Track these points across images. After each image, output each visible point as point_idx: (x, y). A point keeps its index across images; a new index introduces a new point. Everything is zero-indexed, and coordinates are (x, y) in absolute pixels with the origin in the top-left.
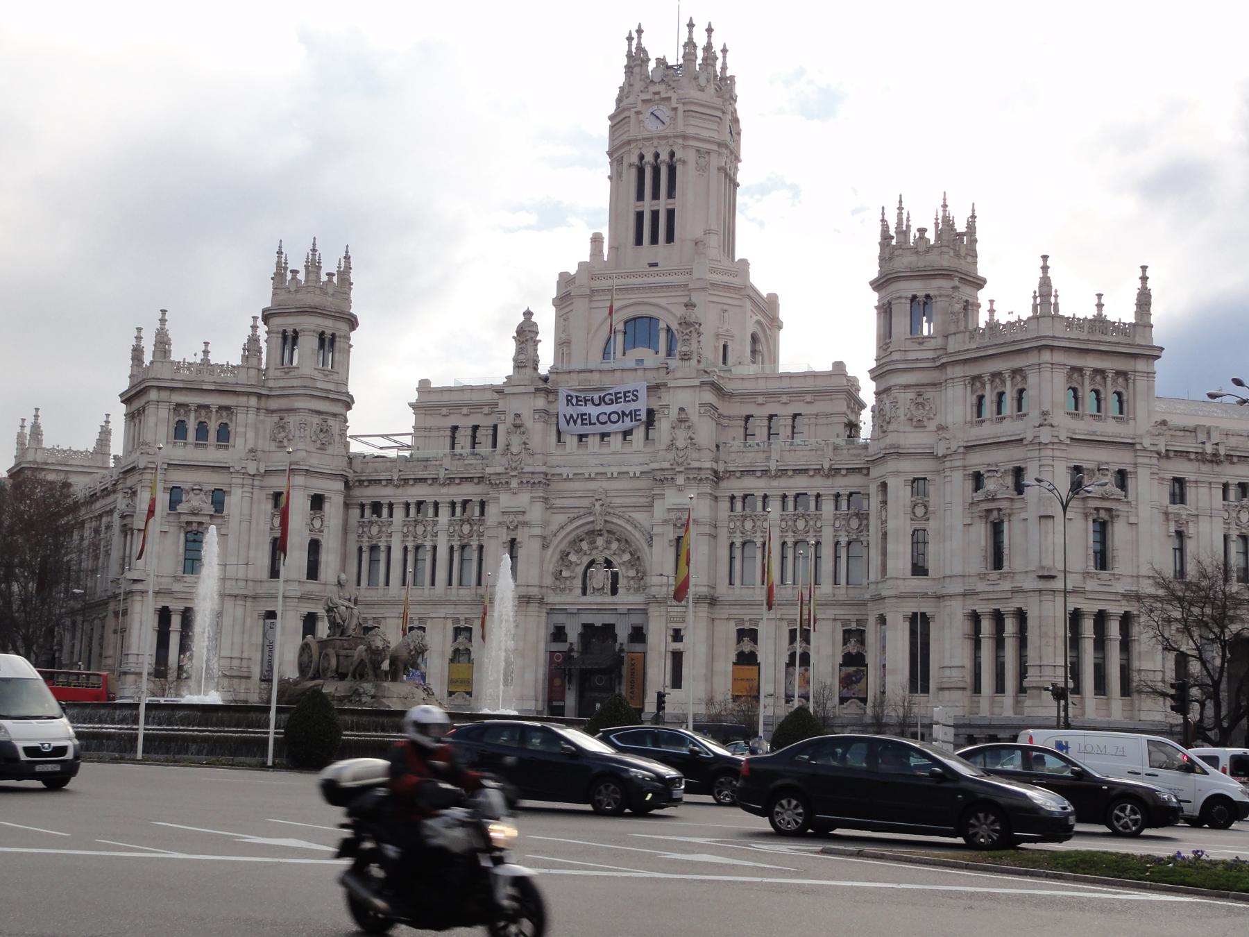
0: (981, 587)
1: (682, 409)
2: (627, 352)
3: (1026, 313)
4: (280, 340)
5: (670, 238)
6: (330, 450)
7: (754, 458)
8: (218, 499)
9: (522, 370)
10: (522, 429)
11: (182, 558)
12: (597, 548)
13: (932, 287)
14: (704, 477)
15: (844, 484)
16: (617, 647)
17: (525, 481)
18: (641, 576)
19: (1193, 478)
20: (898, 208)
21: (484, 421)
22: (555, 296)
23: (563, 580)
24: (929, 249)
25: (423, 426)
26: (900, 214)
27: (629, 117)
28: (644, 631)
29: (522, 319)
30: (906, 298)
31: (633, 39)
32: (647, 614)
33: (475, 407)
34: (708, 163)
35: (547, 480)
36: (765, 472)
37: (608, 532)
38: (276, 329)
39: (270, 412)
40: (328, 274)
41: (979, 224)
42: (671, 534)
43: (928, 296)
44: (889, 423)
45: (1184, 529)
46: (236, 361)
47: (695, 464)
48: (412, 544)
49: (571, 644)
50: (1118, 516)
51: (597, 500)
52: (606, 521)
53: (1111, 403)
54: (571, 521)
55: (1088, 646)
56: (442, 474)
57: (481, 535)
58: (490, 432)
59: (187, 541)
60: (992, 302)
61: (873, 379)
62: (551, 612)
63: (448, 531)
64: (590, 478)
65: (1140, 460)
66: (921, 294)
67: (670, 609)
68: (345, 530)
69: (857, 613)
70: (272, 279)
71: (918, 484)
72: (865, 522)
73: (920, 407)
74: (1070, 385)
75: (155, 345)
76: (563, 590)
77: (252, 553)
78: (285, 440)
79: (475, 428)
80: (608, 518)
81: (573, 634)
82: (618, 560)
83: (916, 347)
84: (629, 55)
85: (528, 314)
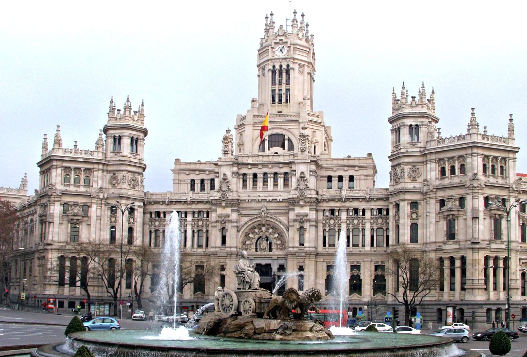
0: (445, 247)
1: (302, 173)
2: (270, 149)
4: (112, 140)
6: (137, 189)
8: (86, 207)
9: (226, 155)
10: (227, 181)
11: (69, 235)
12: (262, 231)
13: (419, 121)
14: (312, 201)
16: (273, 274)
17: (229, 203)
18: (283, 243)
22: (235, 124)
23: (246, 245)
25: (177, 178)
28: (285, 266)
30: (407, 126)
31: (268, 18)
33: (202, 171)
34: (304, 70)
36: (340, 200)
37: (267, 225)
38: (110, 135)
40: (134, 112)
41: (435, 96)
42: (297, 225)
43: (417, 125)
44: (399, 179)
47: (308, 196)
50: (503, 217)
51: (263, 211)
52: (266, 220)
53: (498, 171)
54: (250, 220)
55: (491, 271)
56: (189, 199)
59: (71, 227)
61: (390, 160)
63: (192, 224)
64: (259, 202)
65: (511, 194)
67: (298, 257)
68: (144, 224)
69: (380, 258)
70: (108, 114)
71: (414, 205)
75: (55, 141)
77: (102, 233)
78: (116, 184)
80: (267, 219)
82: (271, 236)
84: (266, 25)
85: (228, 131)
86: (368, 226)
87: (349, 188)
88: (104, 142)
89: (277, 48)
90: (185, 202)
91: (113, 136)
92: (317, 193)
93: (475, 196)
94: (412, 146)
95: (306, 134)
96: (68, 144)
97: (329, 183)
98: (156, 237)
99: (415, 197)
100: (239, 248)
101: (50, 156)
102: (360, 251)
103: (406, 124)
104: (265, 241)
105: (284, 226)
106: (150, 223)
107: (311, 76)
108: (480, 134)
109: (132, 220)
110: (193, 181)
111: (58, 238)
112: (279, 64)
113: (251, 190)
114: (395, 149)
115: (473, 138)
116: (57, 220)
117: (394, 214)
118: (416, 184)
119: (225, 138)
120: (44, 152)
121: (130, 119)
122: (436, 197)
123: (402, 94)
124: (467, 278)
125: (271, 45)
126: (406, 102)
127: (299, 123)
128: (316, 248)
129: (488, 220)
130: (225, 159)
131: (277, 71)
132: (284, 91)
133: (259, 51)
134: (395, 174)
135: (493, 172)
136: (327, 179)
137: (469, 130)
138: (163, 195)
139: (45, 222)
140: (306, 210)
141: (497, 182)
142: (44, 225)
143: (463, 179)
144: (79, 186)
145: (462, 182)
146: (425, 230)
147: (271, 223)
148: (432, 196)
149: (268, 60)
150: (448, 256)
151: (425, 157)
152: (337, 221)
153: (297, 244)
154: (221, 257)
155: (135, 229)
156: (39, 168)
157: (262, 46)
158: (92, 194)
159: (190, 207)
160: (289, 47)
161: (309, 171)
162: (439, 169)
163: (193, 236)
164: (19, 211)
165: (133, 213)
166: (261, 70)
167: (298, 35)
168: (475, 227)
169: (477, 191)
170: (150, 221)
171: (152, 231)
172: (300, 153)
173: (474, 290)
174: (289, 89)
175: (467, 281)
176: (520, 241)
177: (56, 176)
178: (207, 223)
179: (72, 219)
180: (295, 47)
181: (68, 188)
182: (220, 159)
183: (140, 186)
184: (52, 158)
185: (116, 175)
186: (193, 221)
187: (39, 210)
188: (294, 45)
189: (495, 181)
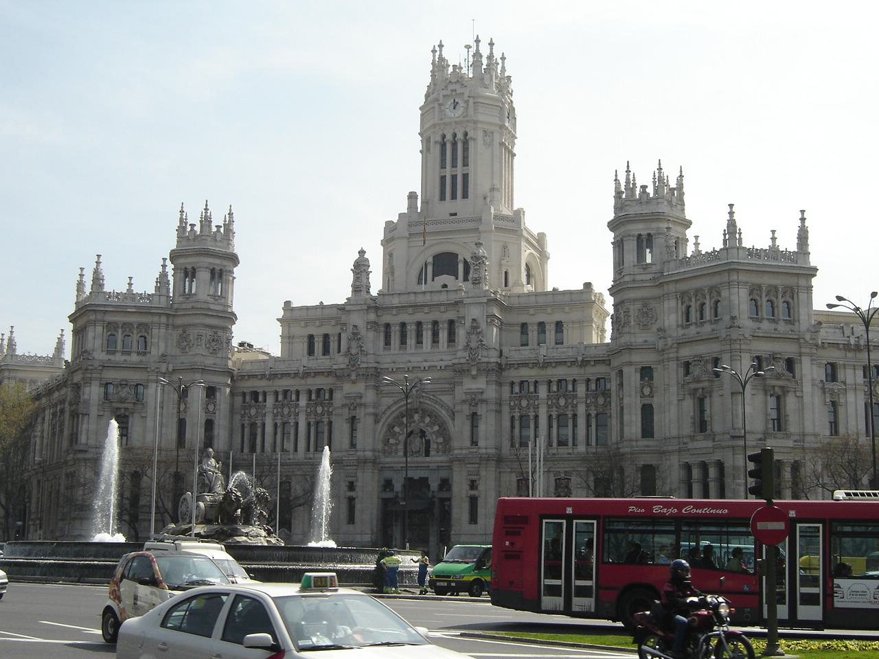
0: (691, 446)
3: (719, 246)
4: (182, 275)
5: (465, 196)
7: (526, 353)
12: (414, 422)
15: (594, 371)
16: (430, 494)
18: (447, 440)
19: (841, 363)
20: (626, 171)
24: (649, 201)
26: (628, 176)
27: (434, 108)
29: (357, 256)
30: (633, 236)
32: (452, 469)
33: (323, 321)
35: (376, 374)
36: (536, 365)
39: (175, 327)
42: (466, 410)
43: (649, 235)
44: (623, 327)
45: (836, 399)
46: (151, 291)
47: (486, 360)
48: (280, 421)
49: (397, 492)
50: (788, 392)
52: (420, 402)
54: (395, 403)
57: (330, 414)
58: (336, 338)
60: (697, 237)
61: (610, 295)
62: (381, 470)
66: (644, 233)
68: (232, 411)
70: (177, 230)
71: (646, 372)
72: (608, 399)
73: (645, 315)
74: (750, 297)
76: (390, 453)
77: (164, 429)
79: (326, 337)
81: (398, 486)
83: (641, 271)
84: (433, 63)
85: (362, 252)
86: (581, 410)
88: (171, 279)
91: (183, 267)
92: (501, 355)
102: (570, 454)
103: (631, 233)
104: (419, 439)
109: (211, 408)
110: (311, 337)
113: (396, 352)
121: (209, 239)
122: (678, 359)
127: (480, 233)
128: (498, 448)
129: (760, 397)
140: (480, 384)
142: (76, 419)
149: (434, 126)
153: (468, 443)
154: (349, 468)
155: (216, 422)
158: (149, 366)
160: (467, 102)
168: (736, 410)
171: (246, 425)
177: (94, 338)
179: (117, 409)
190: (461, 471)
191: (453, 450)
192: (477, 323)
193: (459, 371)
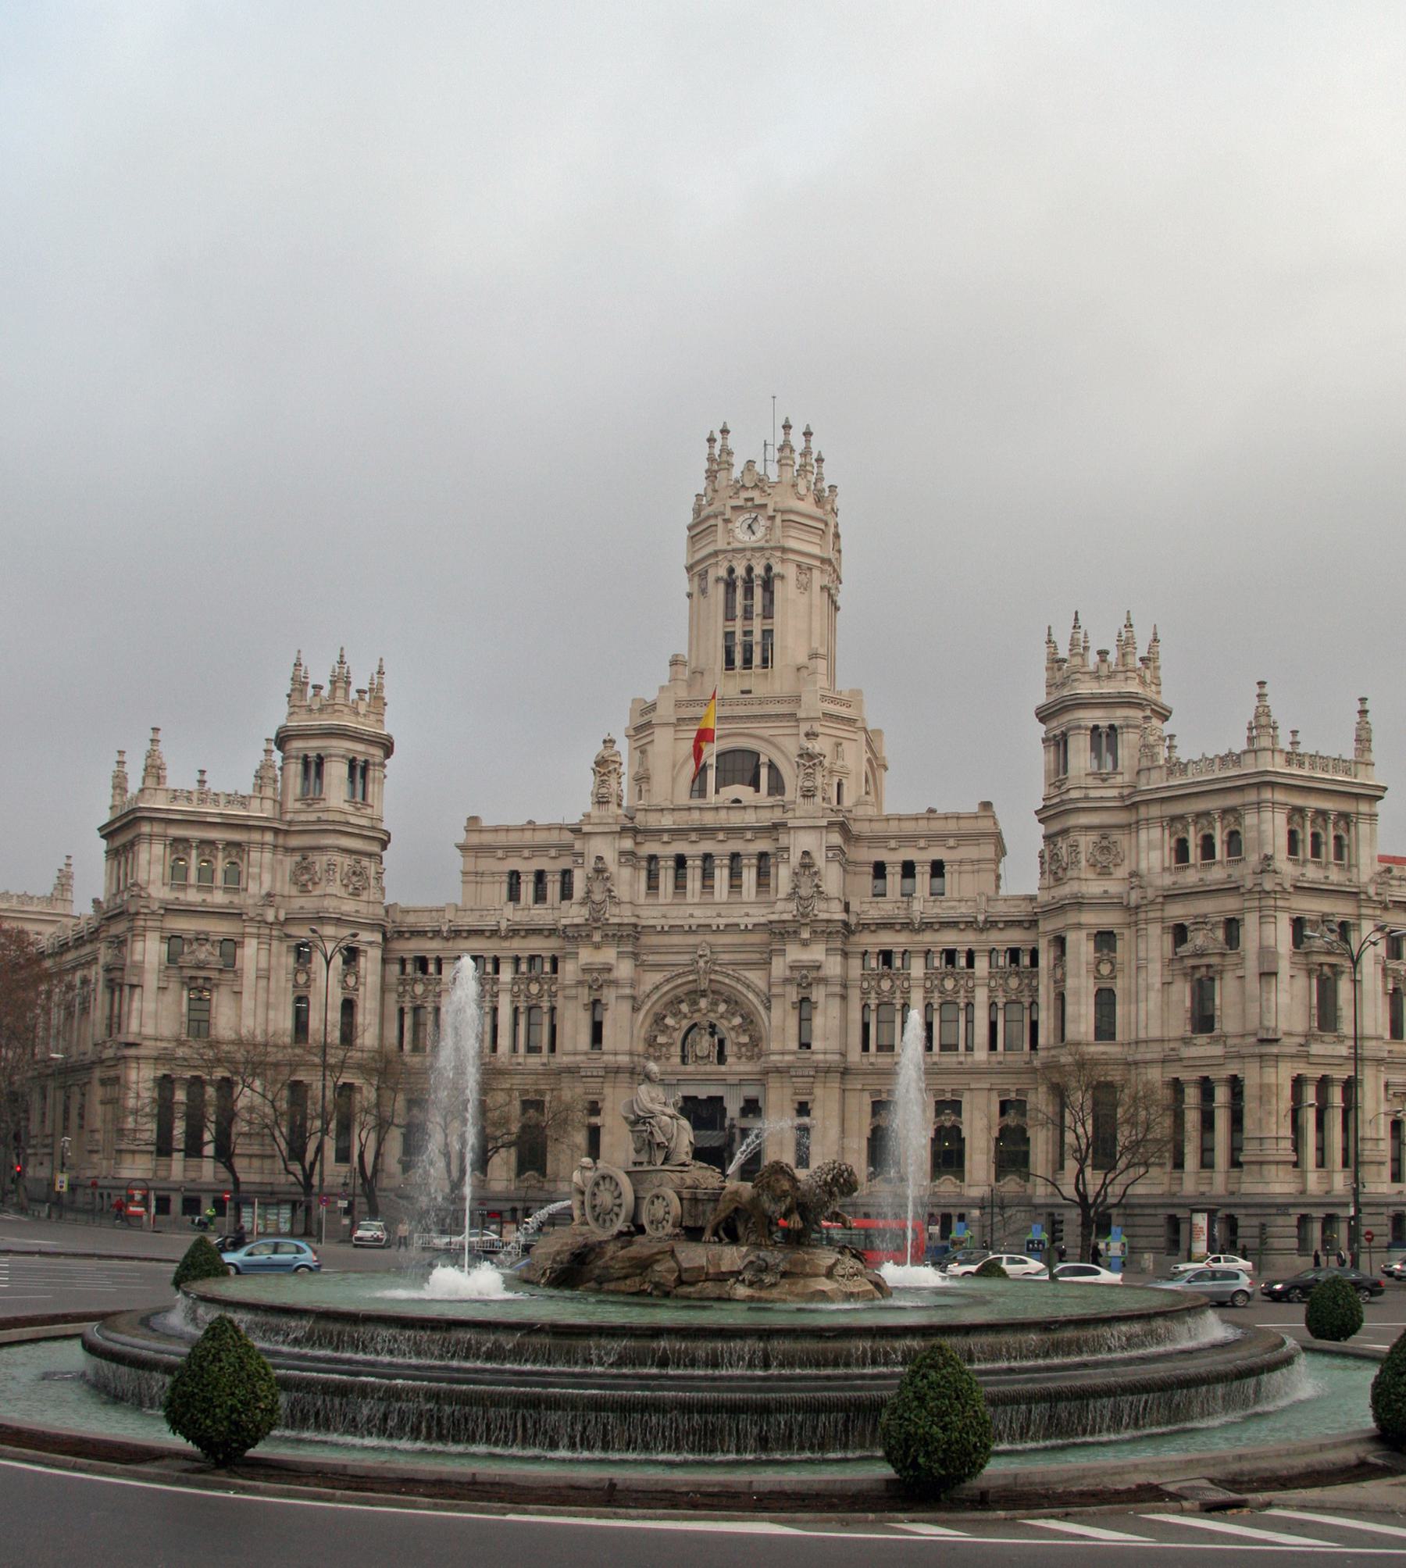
1: (806, 853)
2: (721, 790)
4: (300, 767)
6: (364, 897)
8: (228, 946)
9: (604, 807)
10: (606, 875)
11: (185, 1019)
12: (699, 1010)
13: (1119, 716)
14: (834, 930)
17: (610, 933)
18: (755, 1041)
21: (552, 866)
22: (627, 724)
23: (658, 1047)
25: (472, 869)
28: (760, 1104)
30: (1086, 728)
33: (538, 849)
34: (810, 581)
36: (907, 926)
37: (713, 992)
38: (294, 753)
40: (358, 691)
41: (1162, 648)
42: (793, 994)
43: (1112, 727)
44: (1065, 869)
47: (823, 916)
50: (1343, 972)
51: (701, 956)
52: (711, 981)
53: (1329, 850)
54: (668, 981)
55: (1310, 1117)
56: (504, 925)
57: (553, 995)
59: (190, 999)
61: (1040, 821)
63: (512, 990)
64: (690, 931)
65: (1364, 911)
67: (794, 1080)
69: (1016, 1081)
70: (289, 696)
71: (1105, 939)
75: (145, 770)
77: (272, 1014)
78: (310, 884)
80: (713, 977)
82: (725, 1022)
84: (711, 459)
85: (609, 742)
86: (981, 996)
87: (932, 894)
88: (279, 773)
89: (740, 522)
90: (494, 933)
91: (301, 755)
93: (1269, 916)
94: (1099, 783)
95: (817, 750)
96: (180, 777)
97: (879, 882)
98: (417, 1025)
99: (1108, 919)
100: (639, 1055)
101: (134, 810)
102: (961, 1063)
103: (1083, 724)
104: (707, 1037)
105: (757, 995)
106: (401, 989)
107: (830, 595)
108: (1281, 751)
109: (351, 981)
110: (515, 876)
111: (156, 1028)
112: (745, 563)
113: (669, 901)
114: (1053, 791)
115: (1261, 761)
116: (151, 981)
117: (1052, 964)
118: (1108, 882)
119: (601, 762)
120: (118, 798)
121: (346, 710)
122: (1162, 920)
123: (1074, 644)
124: (1245, 1135)
125: (723, 514)
126: (1083, 666)
127: (797, 720)
128: (843, 1055)
129: (1301, 981)
130: (601, 817)
131: (739, 583)
132: (757, 637)
133: (690, 528)
134: (1055, 858)
135: (1316, 853)
136: (871, 870)
137: (1250, 739)
138: (434, 913)
139: (121, 986)
140: (816, 953)
141: (1327, 877)
142: (117, 994)
143: (1236, 872)
144: (210, 890)
145: (1233, 879)
146: (1133, 1007)
147: (723, 989)
148: (1151, 915)
149: (716, 553)
150: (1196, 1075)
151: (1134, 811)
152: (898, 983)
153: (794, 1045)
154: (589, 1080)
155: (360, 1004)
156: (104, 842)
157: (699, 516)
158: (245, 911)
159: (506, 944)
160: (772, 518)
161: (824, 849)
162: (1170, 843)
163: (516, 1024)
164: (50, 955)
165: (354, 960)
166: (696, 579)
167: (794, 486)
168: (1268, 1000)
169: (1272, 902)
170: (401, 984)
171: (406, 1010)
172: (800, 800)
173: (1265, 1167)
174: (772, 631)
175: (1245, 1142)
176: (1387, 1035)
177: (149, 863)
178: (554, 989)
179: (191, 978)
180: (788, 519)
181: (181, 896)
182: (587, 816)
183: (372, 890)
184: (139, 814)
185: (310, 859)
186: (514, 982)
187: (105, 954)
188: (783, 512)
189: (1321, 876)
190: (782, 1087)
191: (769, 1055)
192: (811, 858)
193: (780, 933)
